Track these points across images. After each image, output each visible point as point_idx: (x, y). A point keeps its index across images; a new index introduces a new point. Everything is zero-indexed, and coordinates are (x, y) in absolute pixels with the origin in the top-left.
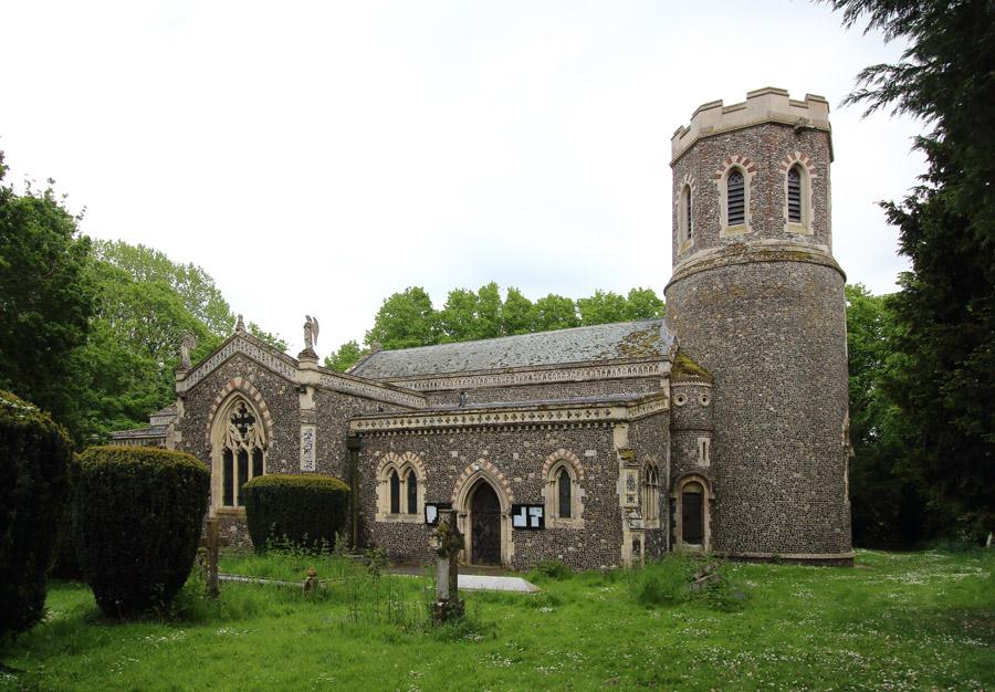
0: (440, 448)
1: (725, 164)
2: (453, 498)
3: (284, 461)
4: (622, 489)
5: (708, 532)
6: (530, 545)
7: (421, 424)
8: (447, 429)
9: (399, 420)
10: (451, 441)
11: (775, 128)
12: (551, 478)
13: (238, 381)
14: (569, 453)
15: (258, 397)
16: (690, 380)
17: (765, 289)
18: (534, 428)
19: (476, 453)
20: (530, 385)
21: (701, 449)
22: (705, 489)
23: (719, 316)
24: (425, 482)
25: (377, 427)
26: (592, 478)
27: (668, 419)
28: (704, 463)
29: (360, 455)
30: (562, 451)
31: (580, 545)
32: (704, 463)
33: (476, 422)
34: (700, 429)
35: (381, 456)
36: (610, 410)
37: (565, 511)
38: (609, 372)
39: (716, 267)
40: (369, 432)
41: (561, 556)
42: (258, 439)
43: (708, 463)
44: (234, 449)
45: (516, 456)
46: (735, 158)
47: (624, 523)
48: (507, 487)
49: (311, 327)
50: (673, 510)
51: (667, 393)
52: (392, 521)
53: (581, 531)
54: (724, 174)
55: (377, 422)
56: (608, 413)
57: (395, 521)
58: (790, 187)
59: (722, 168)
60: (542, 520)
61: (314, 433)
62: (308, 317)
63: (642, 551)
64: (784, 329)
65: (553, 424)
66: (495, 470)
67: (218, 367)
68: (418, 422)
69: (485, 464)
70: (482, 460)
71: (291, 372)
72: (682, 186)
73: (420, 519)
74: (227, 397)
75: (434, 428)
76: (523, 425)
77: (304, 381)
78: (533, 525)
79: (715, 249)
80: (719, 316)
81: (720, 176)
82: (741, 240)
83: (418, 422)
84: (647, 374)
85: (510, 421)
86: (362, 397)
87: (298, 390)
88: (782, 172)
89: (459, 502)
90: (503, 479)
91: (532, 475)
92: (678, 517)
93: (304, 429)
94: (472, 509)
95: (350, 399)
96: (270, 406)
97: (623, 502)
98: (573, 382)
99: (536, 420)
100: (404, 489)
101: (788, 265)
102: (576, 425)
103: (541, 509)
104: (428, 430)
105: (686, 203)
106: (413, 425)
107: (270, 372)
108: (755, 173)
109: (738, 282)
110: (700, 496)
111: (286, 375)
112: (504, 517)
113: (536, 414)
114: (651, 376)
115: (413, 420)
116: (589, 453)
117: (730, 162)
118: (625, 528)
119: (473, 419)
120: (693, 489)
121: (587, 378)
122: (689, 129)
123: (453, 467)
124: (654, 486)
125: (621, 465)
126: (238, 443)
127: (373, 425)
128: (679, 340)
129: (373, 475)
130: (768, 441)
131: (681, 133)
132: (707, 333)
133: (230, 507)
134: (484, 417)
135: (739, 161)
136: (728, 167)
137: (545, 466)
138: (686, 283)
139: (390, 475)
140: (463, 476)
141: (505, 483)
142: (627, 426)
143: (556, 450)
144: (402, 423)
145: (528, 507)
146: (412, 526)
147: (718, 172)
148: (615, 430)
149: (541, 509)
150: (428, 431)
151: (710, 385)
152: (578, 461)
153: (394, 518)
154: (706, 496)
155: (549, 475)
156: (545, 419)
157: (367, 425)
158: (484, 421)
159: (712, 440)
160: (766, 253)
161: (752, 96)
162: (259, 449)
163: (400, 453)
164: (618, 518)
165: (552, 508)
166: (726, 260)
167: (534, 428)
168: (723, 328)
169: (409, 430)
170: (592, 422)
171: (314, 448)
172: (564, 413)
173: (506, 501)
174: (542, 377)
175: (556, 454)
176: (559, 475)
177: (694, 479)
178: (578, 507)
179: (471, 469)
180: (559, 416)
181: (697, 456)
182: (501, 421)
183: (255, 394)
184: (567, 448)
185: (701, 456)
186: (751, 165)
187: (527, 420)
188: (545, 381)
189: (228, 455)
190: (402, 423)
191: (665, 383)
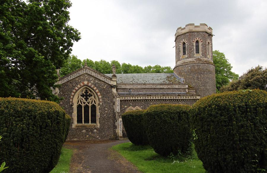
1: (195, 39)
3: (106, 109)
11: (206, 33)
15: (95, 88)
16: (193, 90)
20: (151, 88)
23: (197, 75)
25: (126, 99)
33: (159, 98)
36: (196, 97)
38: (173, 86)
39: (195, 63)
46: (198, 38)
54: (195, 41)
55: (126, 97)
58: (196, 47)
59: (195, 40)
65: (182, 100)
75: (146, 100)
76: (173, 100)
79: (194, 59)
80: (197, 75)
82: (200, 58)
84: (183, 88)
85: (170, 98)
96: (100, 91)
99: (177, 98)
101: (210, 65)
102: (188, 100)
104: (144, 100)
106: (139, 99)
108: (202, 43)
111: (107, 82)
113: (177, 97)
115: (139, 97)
119: (158, 98)
121: (167, 88)
122: (184, 28)
127: (125, 98)
133: (81, 124)
134: (162, 97)
135: (199, 39)
136: (196, 40)
138: (187, 66)
147: (194, 41)
156: (180, 98)
157: (122, 98)
158: (162, 98)
160: (205, 61)
161: (201, 24)
166: (198, 62)
168: (198, 78)
169: (138, 100)
170: (192, 99)
172: (185, 97)
182: (167, 98)
186: (201, 41)
187: (175, 98)
188: (156, 88)
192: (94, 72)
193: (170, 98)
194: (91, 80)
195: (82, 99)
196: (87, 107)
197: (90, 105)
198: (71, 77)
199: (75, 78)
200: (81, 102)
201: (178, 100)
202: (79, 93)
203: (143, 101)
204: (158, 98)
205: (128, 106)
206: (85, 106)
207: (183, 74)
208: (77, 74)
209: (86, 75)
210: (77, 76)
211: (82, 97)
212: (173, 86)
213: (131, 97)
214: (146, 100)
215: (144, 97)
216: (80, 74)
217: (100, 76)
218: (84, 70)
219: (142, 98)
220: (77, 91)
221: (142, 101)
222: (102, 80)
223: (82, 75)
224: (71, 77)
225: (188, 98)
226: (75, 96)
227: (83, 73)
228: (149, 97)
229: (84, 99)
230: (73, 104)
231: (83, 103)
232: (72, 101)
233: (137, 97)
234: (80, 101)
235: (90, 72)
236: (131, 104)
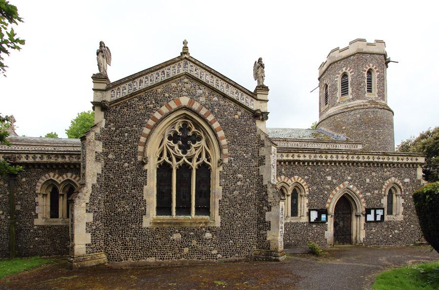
2: (327, 205)
6: (374, 231)
8: (326, 162)
14: (397, 180)
26: (407, 193)
30: (393, 178)
31: (401, 229)
33: (345, 159)
36: (418, 158)
41: (391, 236)
44: (175, 164)
45: (368, 180)
48: (362, 198)
53: (401, 222)
56: (417, 160)
60: (382, 217)
66: (355, 189)
68: (305, 156)
70: (347, 182)
73: (305, 219)
75: (317, 162)
76: (373, 163)
78: (377, 220)
89: (331, 208)
90: (360, 194)
91: (376, 192)
99: (381, 160)
103: (382, 211)
104: (313, 162)
106: (302, 158)
113: (381, 157)
116: (407, 180)
119: (343, 158)
123: (328, 187)
126: (178, 159)
134: (350, 156)
137: (384, 187)
140: (334, 192)
141: (361, 196)
143: (390, 178)
144: (293, 156)
145: (375, 210)
149: (382, 211)
156: (386, 160)
158: (350, 159)
163: (290, 176)
169: (299, 161)
170: (409, 164)
173: (361, 207)
182: (361, 160)
184: (395, 177)
187: (376, 160)
189: (164, 170)
190: (293, 156)
193: (367, 160)
196: (185, 170)
200: (169, 155)
201: (382, 163)
202: (163, 128)
203: (310, 164)
204: (343, 158)
206: (180, 167)
213: (284, 154)
214: (317, 163)
215: (313, 155)
219: (307, 158)
221: (308, 163)
228: (322, 155)
233: (297, 154)
236: (283, 170)
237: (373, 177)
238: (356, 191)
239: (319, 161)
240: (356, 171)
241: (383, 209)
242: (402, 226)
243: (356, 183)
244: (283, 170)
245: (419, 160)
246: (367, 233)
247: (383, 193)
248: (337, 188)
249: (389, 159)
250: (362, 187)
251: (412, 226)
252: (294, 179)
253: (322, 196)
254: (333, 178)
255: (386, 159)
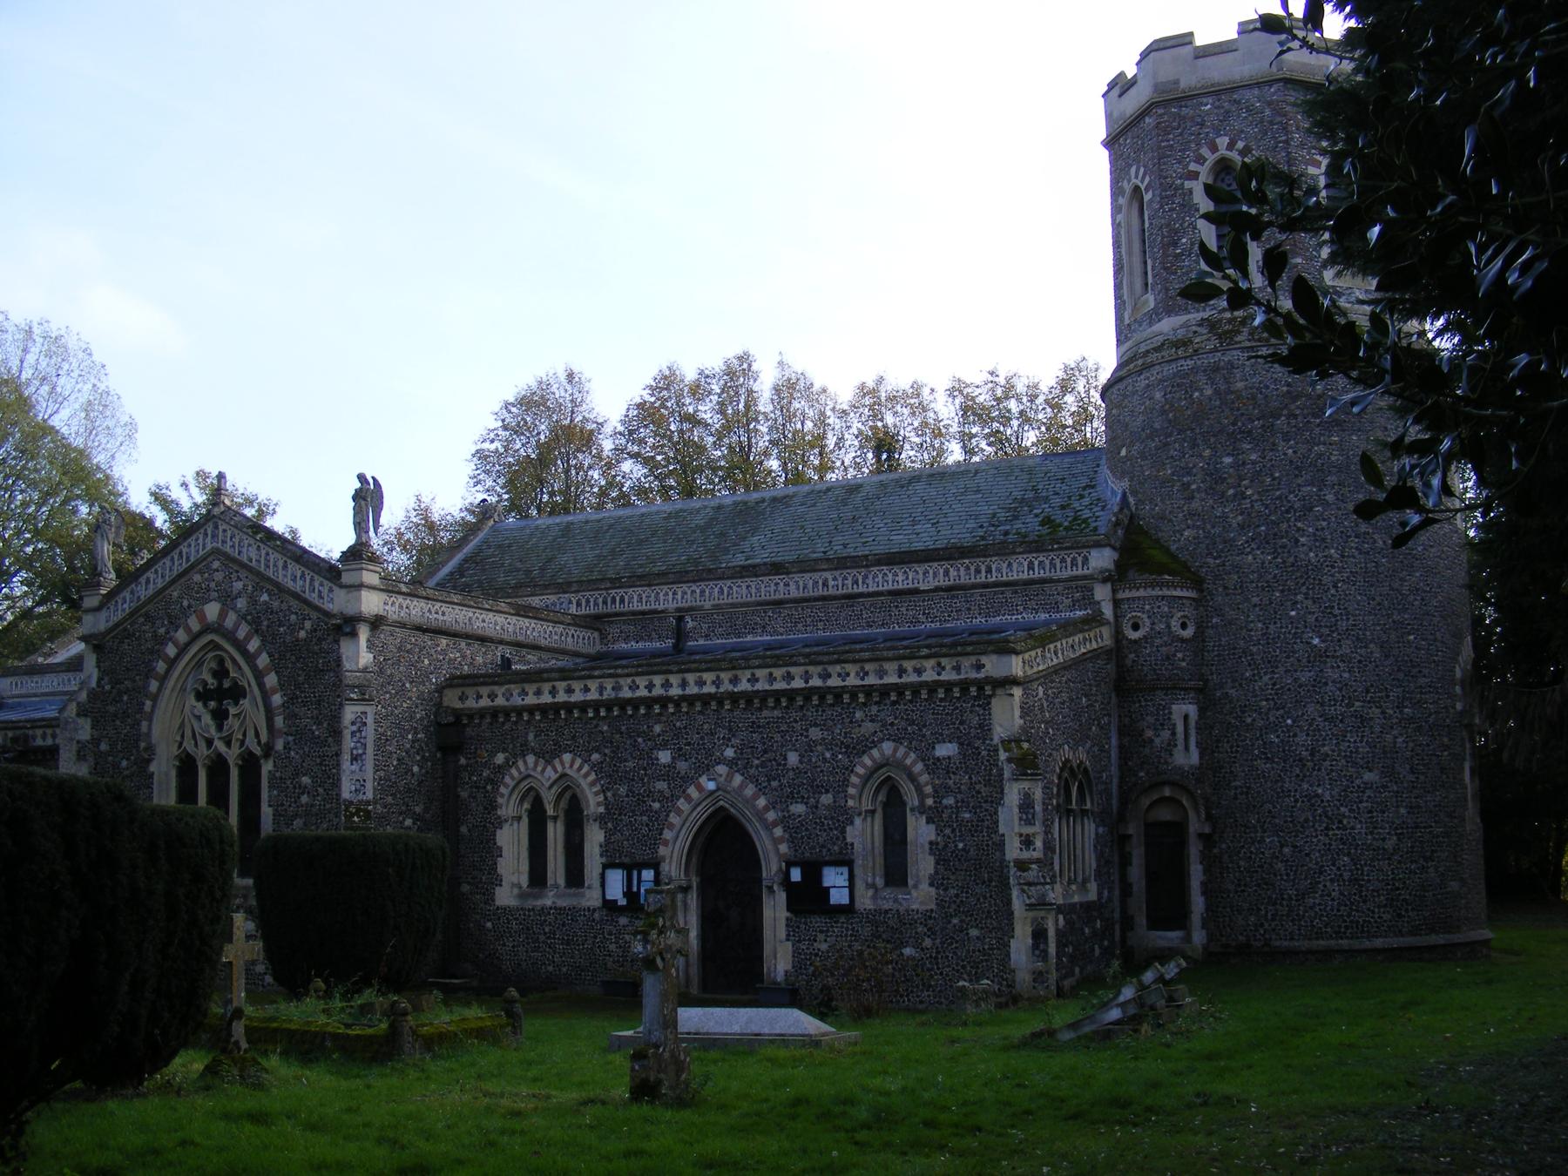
0: (635, 745)
1: (1205, 151)
3: (306, 780)
4: (1009, 820)
5: (1198, 903)
6: (824, 947)
7: (593, 695)
8: (649, 702)
9: (547, 687)
10: (658, 729)
12: (866, 805)
13: (212, 610)
14: (901, 751)
15: (253, 645)
17: (1295, 398)
18: (830, 699)
19: (709, 754)
20: (824, 598)
21: (1180, 728)
22: (1192, 814)
23: (1207, 453)
24: (601, 820)
27: (1111, 667)
28: (1188, 757)
29: (463, 761)
30: (888, 747)
31: (928, 942)
32: (1188, 757)
34: (1174, 688)
35: (507, 765)
36: (984, 660)
37: (896, 874)
38: (989, 571)
40: (482, 713)
42: (250, 734)
43: (1194, 758)
45: (793, 758)
46: (1223, 142)
47: (1015, 893)
48: (775, 824)
49: (368, 497)
50: (1125, 861)
51: (1108, 611)
52: (530, 903)
53: (928, 915)
56: (979, 667)
57: (539, 903)
59: (1200, 160)
61: (370, 720)
62: (361, 477)
63: (1052, 949)
64: (1332, 479)
65: (869, 691)
66: (750, 791)
67: (173, 582)
68: (587, 690)
69: (730, 777)
70: (722, 769)
71: (325, 591)
72: (1127, 187)
73: (592, 899)
74: (188, 645)
75: (623, 704)
76: (808, 693)
77: (350, 610)
80: (1207, 453)
81: (1206, 160)
83: (587, 690)
86: (467, 636)
87: (338, 628)
88: (1312, 170)
89: (674, 851)
90: (766, 809)
91: (826, 799)
92: (1136, 873)
93: (350, 713)
94: (701, 873)
95: (444, 642)
97: (1013, 851)
98: (916, 591)
99: (834, 682)
100: (555, 834)
102: (916, 693)
103: (845, 870)
105: (1135, 221)
106: (577, 697)
107: (279, 589)
109: (1240, 385)
110: (1177, 830)
112: (770, 888)
114: (1076, 578)
116: (945, 750)
117: (1214, 149)
118: (1017, 904)
120: (1165, 814)
122: (1133, 82)
123: (661, 785)
124: (1084, 813)
125: (1007, 775)
127: (492, 696)
128: (1131, 500)
129: (492, 806)
130: (1311, 708)
131: (1119, 86)
132: (1186, 486)
135: (1231, 146)
136: (1211, 158)
137: (854, 779)
138: (1142, 382)
139: (526, 806)
140: (682, 804)
141: (771, 816)
142: (1017, 692)
143: (875, 744)
144: (553, 692)
146: (574, 911)
147: (1193, 167)
148: (994, 701)
149: (845, 870)
150: (609, 709)
151: (1192, 594)
152: (919, 767)
153: (536, 897)
154: (1195, 825)
155: (861, 798)
156: (852, 681)
157: (479, 697)
159: (1202, 711)
162: (251, 753)
164: (1005, 886)
165: (870, 868)
167: (830, 699)
168: (1215, 477)
169: (569, 707)
170: (948, 686)
171: (370, 750)
174: (849, 582)
175: (875, 752)
176: (881, 797)
177: (1167, 792)
178: (922, 865)
179: (700, 788)
180: (881, 673)
181: (1172, 744)
183: (248, 638)
185: (1181, 747)
187: (816, 682)
190: (553, 692)
191: (1102, 593)
192: (252, 542)
194: (239, 595)
195: (199, 718)
196: (218, 767)
197: (232, 755)
198: (148, 581)
199: (164, 588)
201: (838, 693)
205: (515, 756)
206: (213, 761)
207: (1123, 452)
208: (176, 557)
209: (216, 564)
210: (175, 573)
211: (200, 705)
212: (989, 571)
214: (623, 708)
216: (188, 559)
217: (281, 564)
218: (209, 532)
220: (172, 663)
221: (597, 711)
222: (290, 584)
223: (198, 562)
224: (148, 581)
225: (919, 672)
226: (162, 704)
227: (201, 553)
229: (207, 719)
230: (150, 749)
231: (202, 744)
232: (149, 734)
234: (188, 733)
235: (236, 540)
236: (531, 737)
237: (810, 746)
238: (755, 797)
239: (629, 701)
240: (754, 727)
241: (849, 863)
242: (932, 933)
243: (752, 771)
244: (531, 737)
245: (988, 667)
246: (796, 953)
247: (851, 803)
248: (692, 791)
249: (866, 674)
250: (775, 784)
251: (974, 932)
252: (562, 763)
253: (645, 818)
254: (679, 754)
255: (852, 675)
